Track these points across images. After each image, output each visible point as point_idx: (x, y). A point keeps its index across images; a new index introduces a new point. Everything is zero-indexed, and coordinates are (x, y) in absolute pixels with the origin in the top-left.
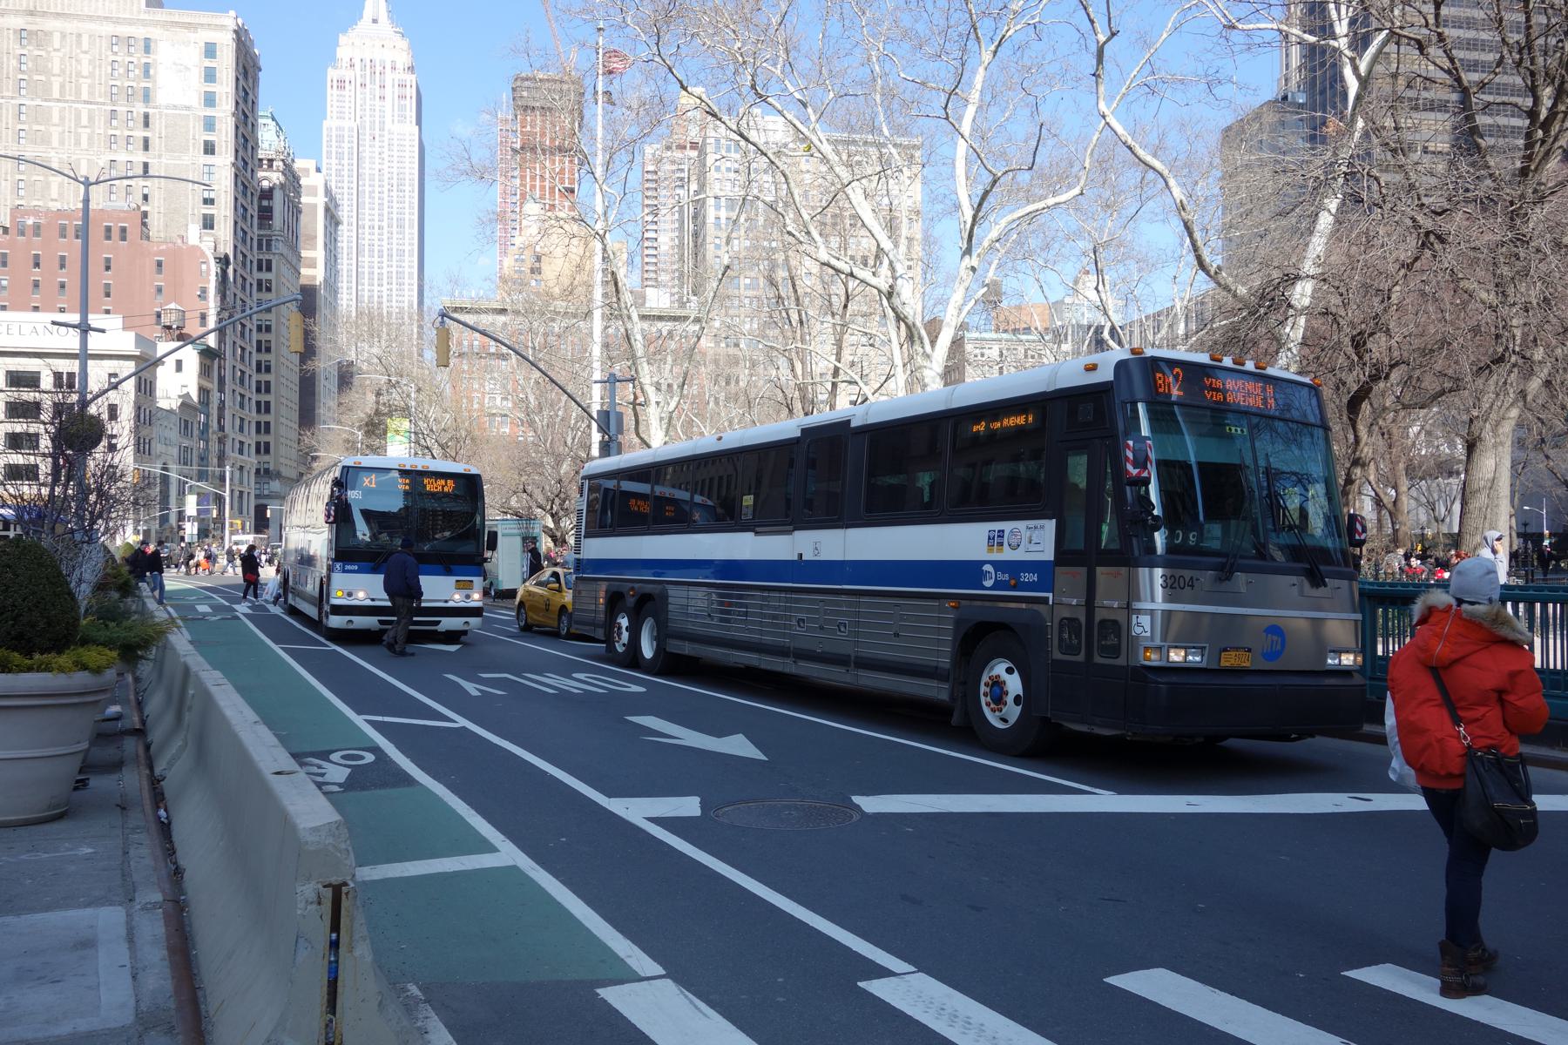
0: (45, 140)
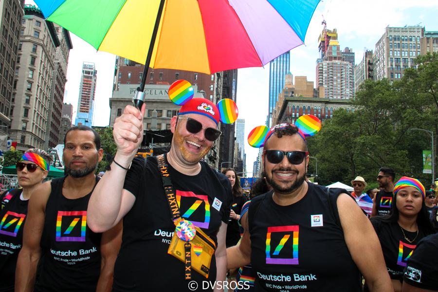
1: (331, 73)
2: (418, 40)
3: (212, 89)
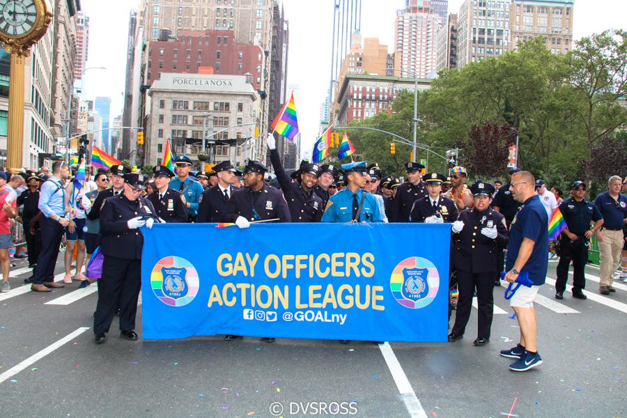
1: (414, 30)
2: (507, 7)
3: (259, 70)
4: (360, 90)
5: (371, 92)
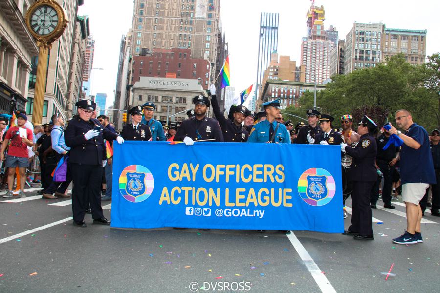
0: (162, 28)
2: (379, 35)
3: (207, 76)
4: (277, 91)
5: (284, 93)
